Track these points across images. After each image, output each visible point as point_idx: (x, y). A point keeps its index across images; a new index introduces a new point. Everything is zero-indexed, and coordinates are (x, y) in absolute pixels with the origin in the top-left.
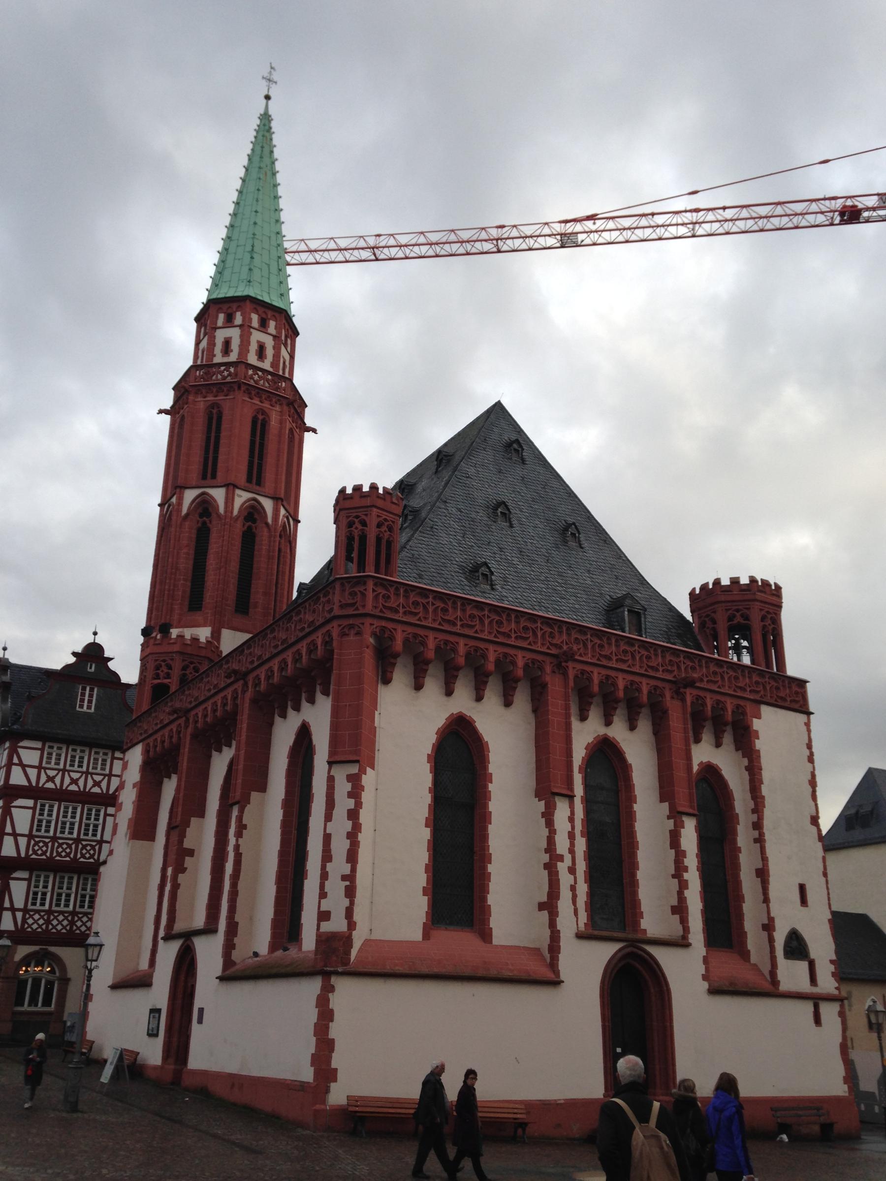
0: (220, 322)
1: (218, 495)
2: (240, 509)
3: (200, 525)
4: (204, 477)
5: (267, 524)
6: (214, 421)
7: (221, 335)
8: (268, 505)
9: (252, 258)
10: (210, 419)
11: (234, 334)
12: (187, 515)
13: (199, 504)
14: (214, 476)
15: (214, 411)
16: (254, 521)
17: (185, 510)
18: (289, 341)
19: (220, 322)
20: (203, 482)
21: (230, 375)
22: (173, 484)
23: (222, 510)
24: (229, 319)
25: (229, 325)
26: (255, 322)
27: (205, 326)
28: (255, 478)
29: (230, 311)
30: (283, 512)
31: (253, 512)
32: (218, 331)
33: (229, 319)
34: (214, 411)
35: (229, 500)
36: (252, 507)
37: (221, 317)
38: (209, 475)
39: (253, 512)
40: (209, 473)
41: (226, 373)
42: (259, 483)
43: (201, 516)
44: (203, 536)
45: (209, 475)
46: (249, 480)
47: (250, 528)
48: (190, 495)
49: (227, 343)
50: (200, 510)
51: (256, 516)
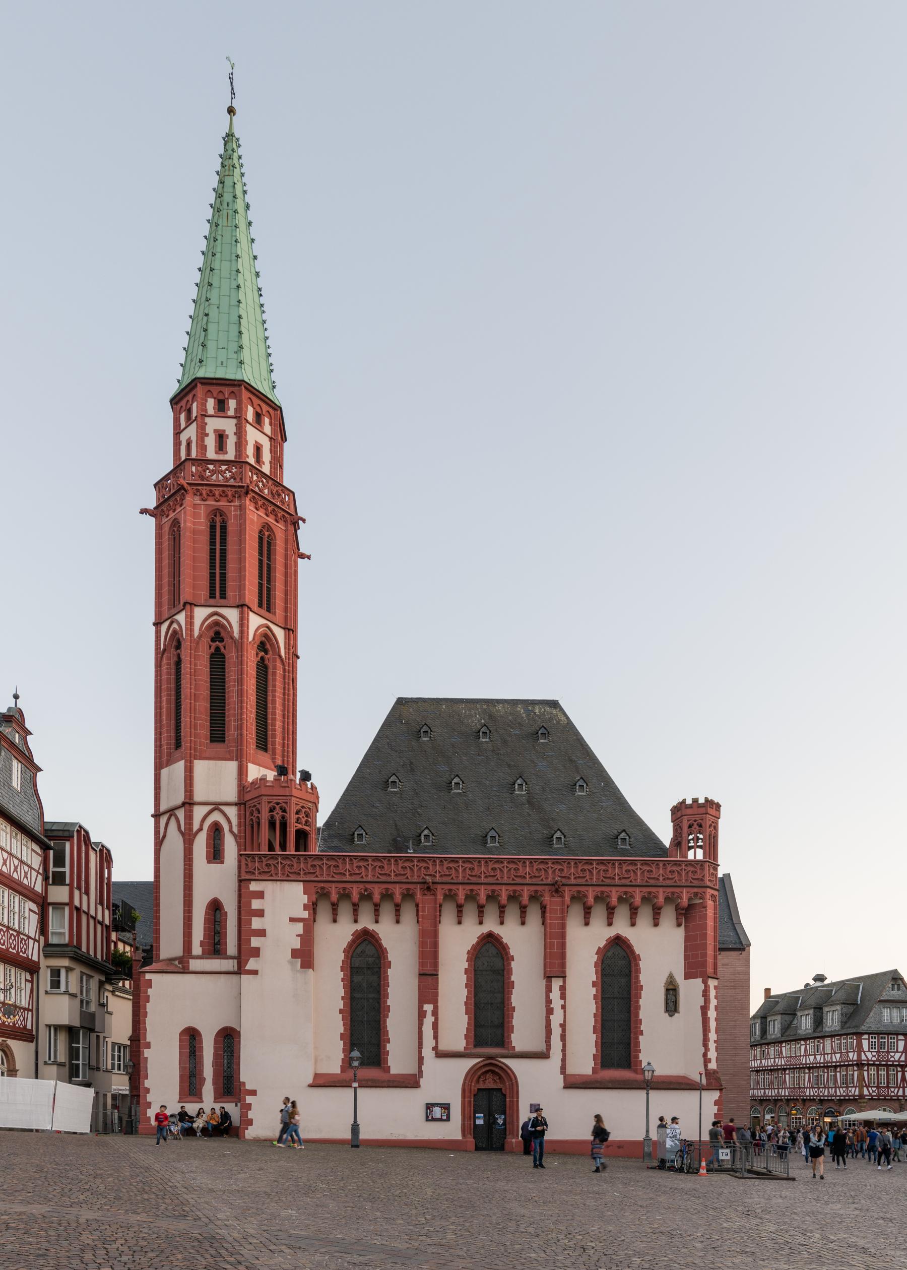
0: (211, 410)
1: (232, 615)
4: (212, 595)
6: (219, 532)
7: (213, 424)
9: (240, 332)
10: (213, 527)
11: (228, 426)
12: (200, 636)
13: (210, 627)
14: (223, 596)
15: (218, 519)
17: (196, 633)
19: (211, 410)
20: (212, 601)
21: (232, 477)
22: (170, 597)
23: (236, 634)
24: (221, 406)
25: (221, 414)
26: (250, 414)
27: (189, 411)
29: (221, 397)
32: (207, 420)
33: (221, 406)
34: (218, 519)
35: (243, 623)
37: (211, 404)
38: (218, 594)
40: (218, 589)
41: (228, 474)
45: (218, 594)
48: (200, 614)
49: (221, 437)
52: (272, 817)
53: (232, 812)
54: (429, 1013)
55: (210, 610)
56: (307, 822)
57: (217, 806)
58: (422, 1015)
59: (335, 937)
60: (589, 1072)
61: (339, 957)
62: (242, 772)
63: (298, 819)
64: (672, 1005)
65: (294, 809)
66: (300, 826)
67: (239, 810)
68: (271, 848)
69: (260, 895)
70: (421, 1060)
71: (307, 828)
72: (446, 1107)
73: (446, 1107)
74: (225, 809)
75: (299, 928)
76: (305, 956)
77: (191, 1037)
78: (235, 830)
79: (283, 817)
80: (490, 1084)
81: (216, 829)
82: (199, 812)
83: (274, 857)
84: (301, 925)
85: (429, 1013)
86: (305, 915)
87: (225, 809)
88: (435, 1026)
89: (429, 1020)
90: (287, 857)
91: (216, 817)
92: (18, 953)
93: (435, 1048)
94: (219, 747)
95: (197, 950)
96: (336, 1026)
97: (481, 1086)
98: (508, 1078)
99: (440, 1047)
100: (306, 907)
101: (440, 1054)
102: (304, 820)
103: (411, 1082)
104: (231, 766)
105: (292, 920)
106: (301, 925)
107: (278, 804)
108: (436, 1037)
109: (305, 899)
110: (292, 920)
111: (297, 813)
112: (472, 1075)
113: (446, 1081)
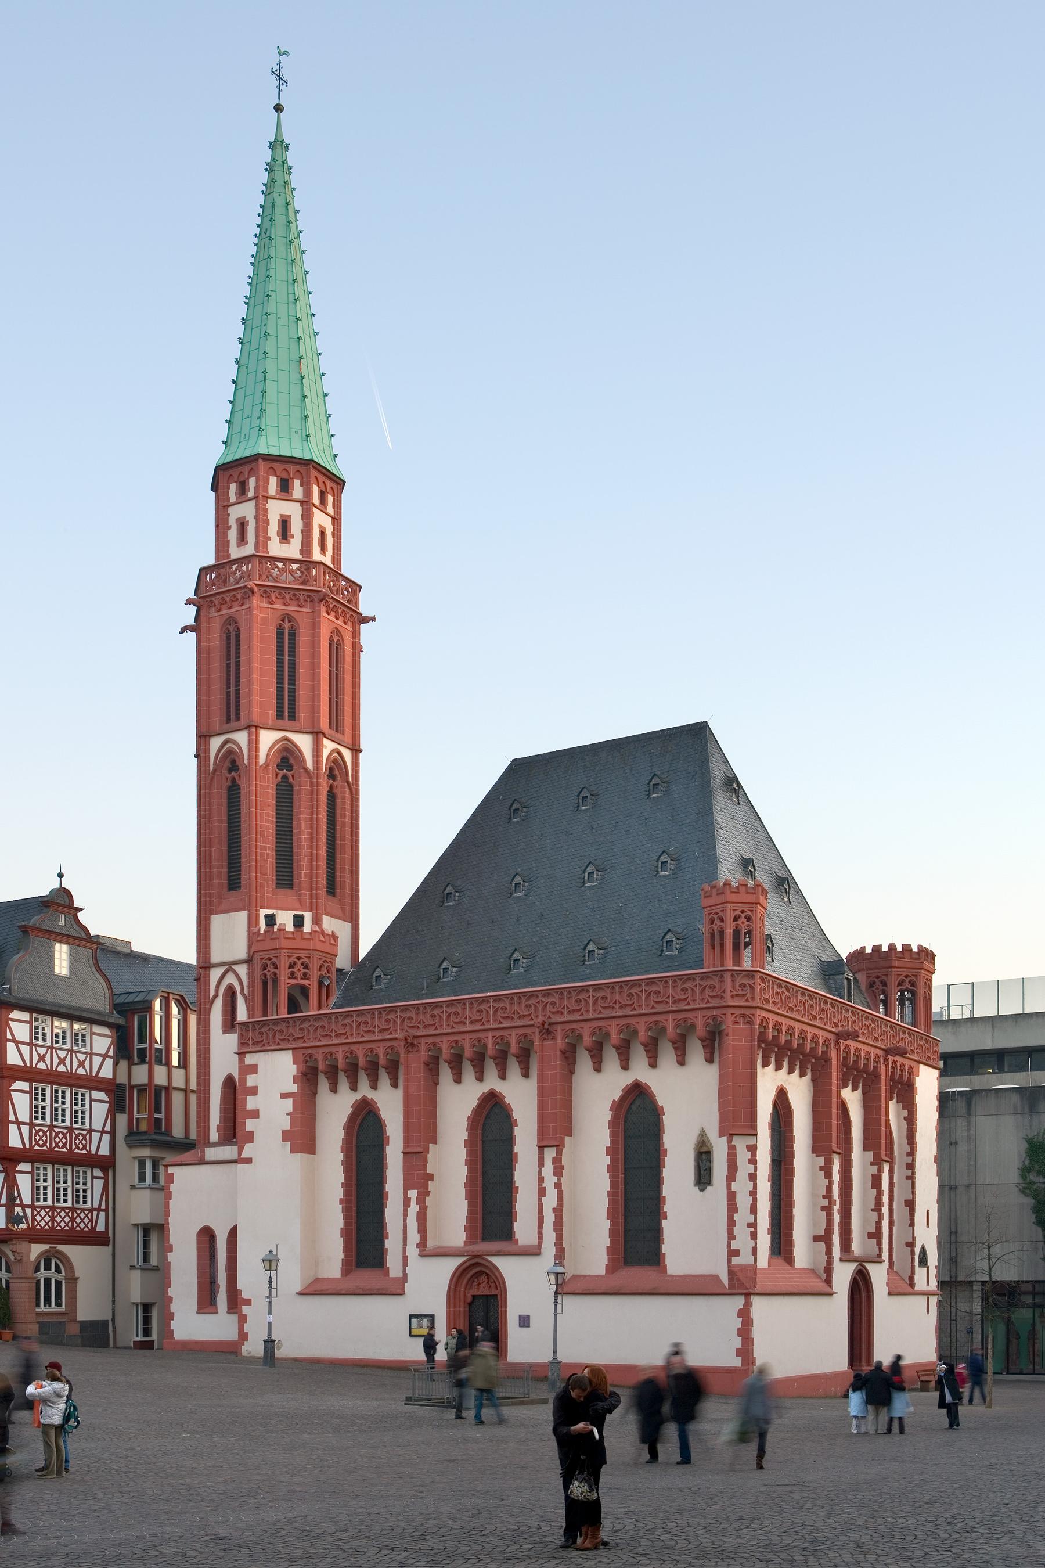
2: (268, 754)
3: (229, 783)
5: (306, 769)
8: (304, 742)
12: (215, 770)
16: (290, 768)
18: (330, 499)
28: (286, 710)
30: (328, 746)
31: (287, 757)
36: (286, 749)
39: (287, 757)
42: (293, 717)
43: (230, 771)
44: (234, 792)
46: (280, 715)
47: (285, 777)
50: (228, 764)
51: (292, 761)
52: (265, 976)
53: (242, 970)
54: (413, 1201)
55: (223, 738)
56: (305, 974)
57: (229, 967)
58: (407, 1203)
59: (335, 1109)
60: (601, 1271)
61: (340, 1134)
62: (252, 921)
63: (292, 974)
64: (703, 1178)
65: (284, 963)
66: (293, 981)
67: (248, 969)
68: (265, 1014)
69: (253, 1069)
70: (405, 1259)
71: (305, 982)
72: (431, 1318)
73: (431, 1318)
74: (235, 967)
75: (288, 1104)
76: (302, 1137)
77: (207, 1235)
78: (246, 992)
79: (275, 974)
80: (483, 1290)
81: (231, 995)
82: (215, 974)
83: (265, 1023)
84: (289, 1102)
85: (413, 1201)
86: (294, 1088)
87: (235, 967)
88: (422, 1217)
89: (414, 1209)
90: (276, 1022)
91: (230, 979)
92: (70, 1150)
93: (422, 1245)
94: (235, 896)
95: (214, 1136)
96: (333, 1219)
97: (474, 1292)
98: (496, 1280)
99: (430, 1244)
100: (295, 1080)
101: (425, 1251)
102: (299, 975)
103: (396, 1289)
104: (243, 915)
105: (284, 1096)
106: (289, 1102)
107: (270, 959)
108: (423, 1231)
109: (293, 1070)
110: (284, 1096)
111: (290, 967)
112: (458, 1278)
113: (429, 1287)
